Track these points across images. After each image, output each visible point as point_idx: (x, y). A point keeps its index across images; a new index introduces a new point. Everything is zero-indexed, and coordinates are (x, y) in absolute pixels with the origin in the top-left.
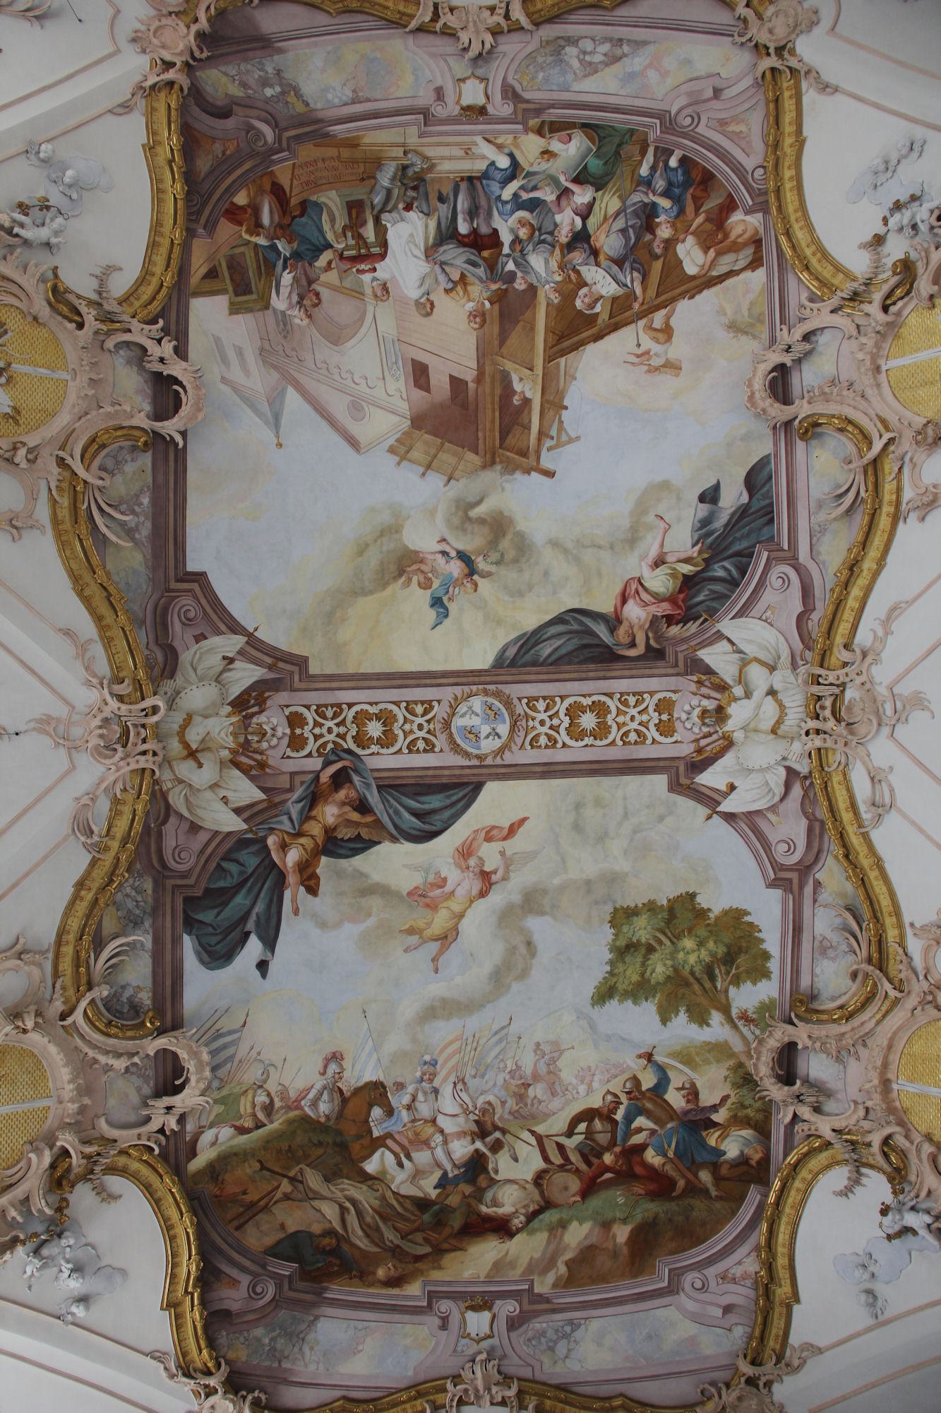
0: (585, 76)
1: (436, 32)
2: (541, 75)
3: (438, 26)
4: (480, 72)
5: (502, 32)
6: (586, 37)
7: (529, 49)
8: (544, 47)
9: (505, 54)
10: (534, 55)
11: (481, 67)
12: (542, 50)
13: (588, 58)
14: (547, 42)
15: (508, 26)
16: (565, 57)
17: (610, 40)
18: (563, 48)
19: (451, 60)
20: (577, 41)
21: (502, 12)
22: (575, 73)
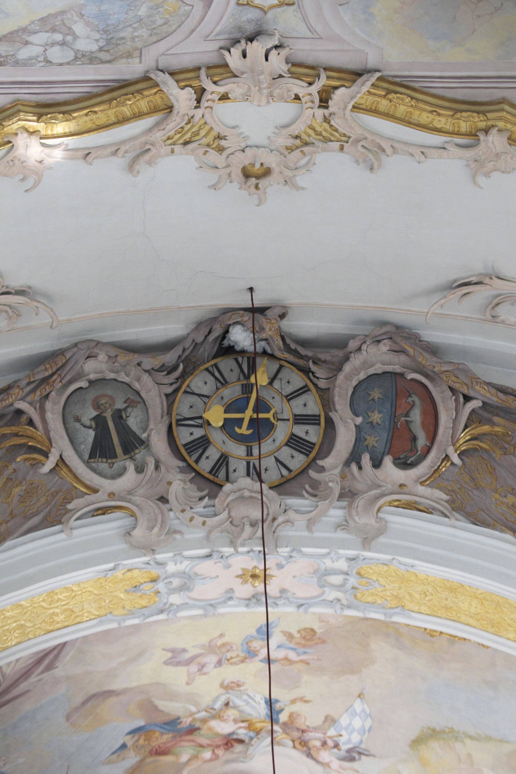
0: (63, 12)
1: (325, 69)
2: (143, 11)
3: (323, 81)
4: (252, 14)
5: (209, 68)
6: (61, 64)
7: (162, 46)
8: (136, 49)
9: (206, 38)
10: (154, 39)
11: (249, 21)
12: (139, 45)
13: (58, 37)
14: (129, 55)
15: (198, 77)
16: (98, 36)
17: (17, 63)
18: (101, 49)
19: (302, 30)
20: (76, 58)
21: (207, 96)
22: (82, 15)
